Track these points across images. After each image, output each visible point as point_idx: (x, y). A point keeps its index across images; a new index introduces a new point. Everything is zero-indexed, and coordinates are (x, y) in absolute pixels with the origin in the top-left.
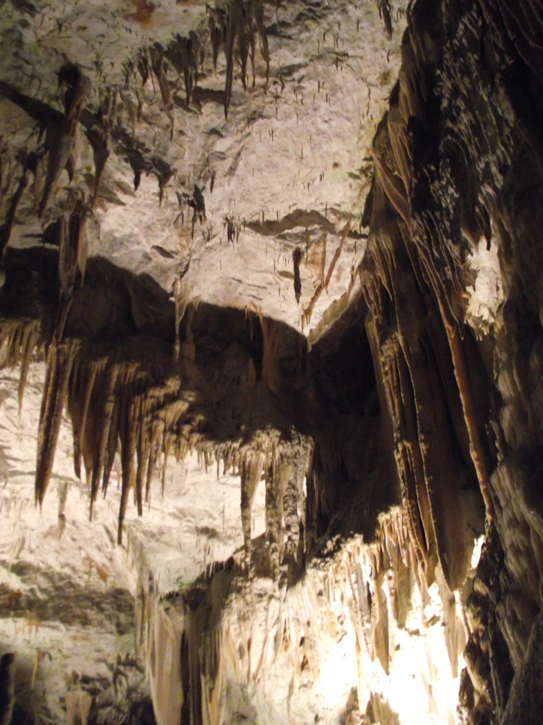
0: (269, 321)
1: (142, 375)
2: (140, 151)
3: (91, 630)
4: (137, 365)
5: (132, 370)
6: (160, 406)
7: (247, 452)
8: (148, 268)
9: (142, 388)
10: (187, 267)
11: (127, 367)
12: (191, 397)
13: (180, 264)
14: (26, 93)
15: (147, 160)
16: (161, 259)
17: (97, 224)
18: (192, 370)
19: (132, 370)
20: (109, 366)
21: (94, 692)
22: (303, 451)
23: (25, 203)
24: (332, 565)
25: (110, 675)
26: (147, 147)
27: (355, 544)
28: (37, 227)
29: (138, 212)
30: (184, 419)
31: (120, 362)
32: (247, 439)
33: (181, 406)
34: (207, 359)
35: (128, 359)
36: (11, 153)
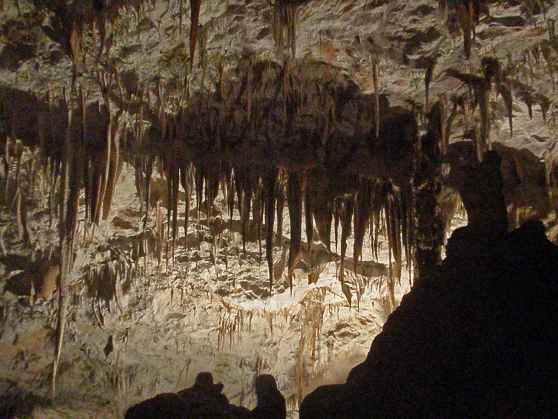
1: (534, 213)
2: (529, 92)
4: (531, 208)
5: (528, 211)
8: (527, 146)
10: (554, 145)
11: (525, 209)
13: (549, 144)
14: (463, 72)
15: (534, 96)
16: (538, 143)
17: (497, 127)
19: (528, 211)
20: (514, 209)
23: (455, 121)
26: (533, 88)
28: (461, 132)
29: (524, 120)
31: (520, 207)
35: (523, 205)
36: (448, 98)
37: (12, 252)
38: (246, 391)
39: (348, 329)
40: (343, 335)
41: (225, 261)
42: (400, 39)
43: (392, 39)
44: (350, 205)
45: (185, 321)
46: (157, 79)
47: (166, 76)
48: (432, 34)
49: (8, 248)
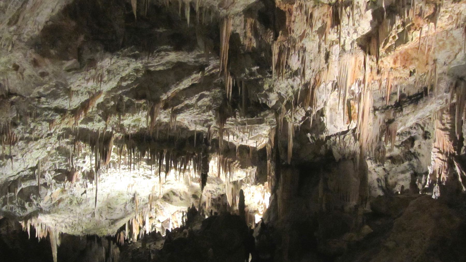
0: (251, 147)
3: (213, 185)
6: (235, 165)
7: (247, 170)
9: (232, 162)
12: (239, 162)
18: (239, 157)
21: (212, 193)
22: (255, 169)
25: (215, 191)
27: (261, 185)
30: (238, 166)
32: (247, 168)
33: (238, 164)
37: (60, 168)
38: (128, 202)
40: (168, 184)
41: (139, 169)
42: (203, 120)
43: (200, 121)
44: (183, 159)
46: (129, 125)
47: (133, 124)
48: (211, 120)
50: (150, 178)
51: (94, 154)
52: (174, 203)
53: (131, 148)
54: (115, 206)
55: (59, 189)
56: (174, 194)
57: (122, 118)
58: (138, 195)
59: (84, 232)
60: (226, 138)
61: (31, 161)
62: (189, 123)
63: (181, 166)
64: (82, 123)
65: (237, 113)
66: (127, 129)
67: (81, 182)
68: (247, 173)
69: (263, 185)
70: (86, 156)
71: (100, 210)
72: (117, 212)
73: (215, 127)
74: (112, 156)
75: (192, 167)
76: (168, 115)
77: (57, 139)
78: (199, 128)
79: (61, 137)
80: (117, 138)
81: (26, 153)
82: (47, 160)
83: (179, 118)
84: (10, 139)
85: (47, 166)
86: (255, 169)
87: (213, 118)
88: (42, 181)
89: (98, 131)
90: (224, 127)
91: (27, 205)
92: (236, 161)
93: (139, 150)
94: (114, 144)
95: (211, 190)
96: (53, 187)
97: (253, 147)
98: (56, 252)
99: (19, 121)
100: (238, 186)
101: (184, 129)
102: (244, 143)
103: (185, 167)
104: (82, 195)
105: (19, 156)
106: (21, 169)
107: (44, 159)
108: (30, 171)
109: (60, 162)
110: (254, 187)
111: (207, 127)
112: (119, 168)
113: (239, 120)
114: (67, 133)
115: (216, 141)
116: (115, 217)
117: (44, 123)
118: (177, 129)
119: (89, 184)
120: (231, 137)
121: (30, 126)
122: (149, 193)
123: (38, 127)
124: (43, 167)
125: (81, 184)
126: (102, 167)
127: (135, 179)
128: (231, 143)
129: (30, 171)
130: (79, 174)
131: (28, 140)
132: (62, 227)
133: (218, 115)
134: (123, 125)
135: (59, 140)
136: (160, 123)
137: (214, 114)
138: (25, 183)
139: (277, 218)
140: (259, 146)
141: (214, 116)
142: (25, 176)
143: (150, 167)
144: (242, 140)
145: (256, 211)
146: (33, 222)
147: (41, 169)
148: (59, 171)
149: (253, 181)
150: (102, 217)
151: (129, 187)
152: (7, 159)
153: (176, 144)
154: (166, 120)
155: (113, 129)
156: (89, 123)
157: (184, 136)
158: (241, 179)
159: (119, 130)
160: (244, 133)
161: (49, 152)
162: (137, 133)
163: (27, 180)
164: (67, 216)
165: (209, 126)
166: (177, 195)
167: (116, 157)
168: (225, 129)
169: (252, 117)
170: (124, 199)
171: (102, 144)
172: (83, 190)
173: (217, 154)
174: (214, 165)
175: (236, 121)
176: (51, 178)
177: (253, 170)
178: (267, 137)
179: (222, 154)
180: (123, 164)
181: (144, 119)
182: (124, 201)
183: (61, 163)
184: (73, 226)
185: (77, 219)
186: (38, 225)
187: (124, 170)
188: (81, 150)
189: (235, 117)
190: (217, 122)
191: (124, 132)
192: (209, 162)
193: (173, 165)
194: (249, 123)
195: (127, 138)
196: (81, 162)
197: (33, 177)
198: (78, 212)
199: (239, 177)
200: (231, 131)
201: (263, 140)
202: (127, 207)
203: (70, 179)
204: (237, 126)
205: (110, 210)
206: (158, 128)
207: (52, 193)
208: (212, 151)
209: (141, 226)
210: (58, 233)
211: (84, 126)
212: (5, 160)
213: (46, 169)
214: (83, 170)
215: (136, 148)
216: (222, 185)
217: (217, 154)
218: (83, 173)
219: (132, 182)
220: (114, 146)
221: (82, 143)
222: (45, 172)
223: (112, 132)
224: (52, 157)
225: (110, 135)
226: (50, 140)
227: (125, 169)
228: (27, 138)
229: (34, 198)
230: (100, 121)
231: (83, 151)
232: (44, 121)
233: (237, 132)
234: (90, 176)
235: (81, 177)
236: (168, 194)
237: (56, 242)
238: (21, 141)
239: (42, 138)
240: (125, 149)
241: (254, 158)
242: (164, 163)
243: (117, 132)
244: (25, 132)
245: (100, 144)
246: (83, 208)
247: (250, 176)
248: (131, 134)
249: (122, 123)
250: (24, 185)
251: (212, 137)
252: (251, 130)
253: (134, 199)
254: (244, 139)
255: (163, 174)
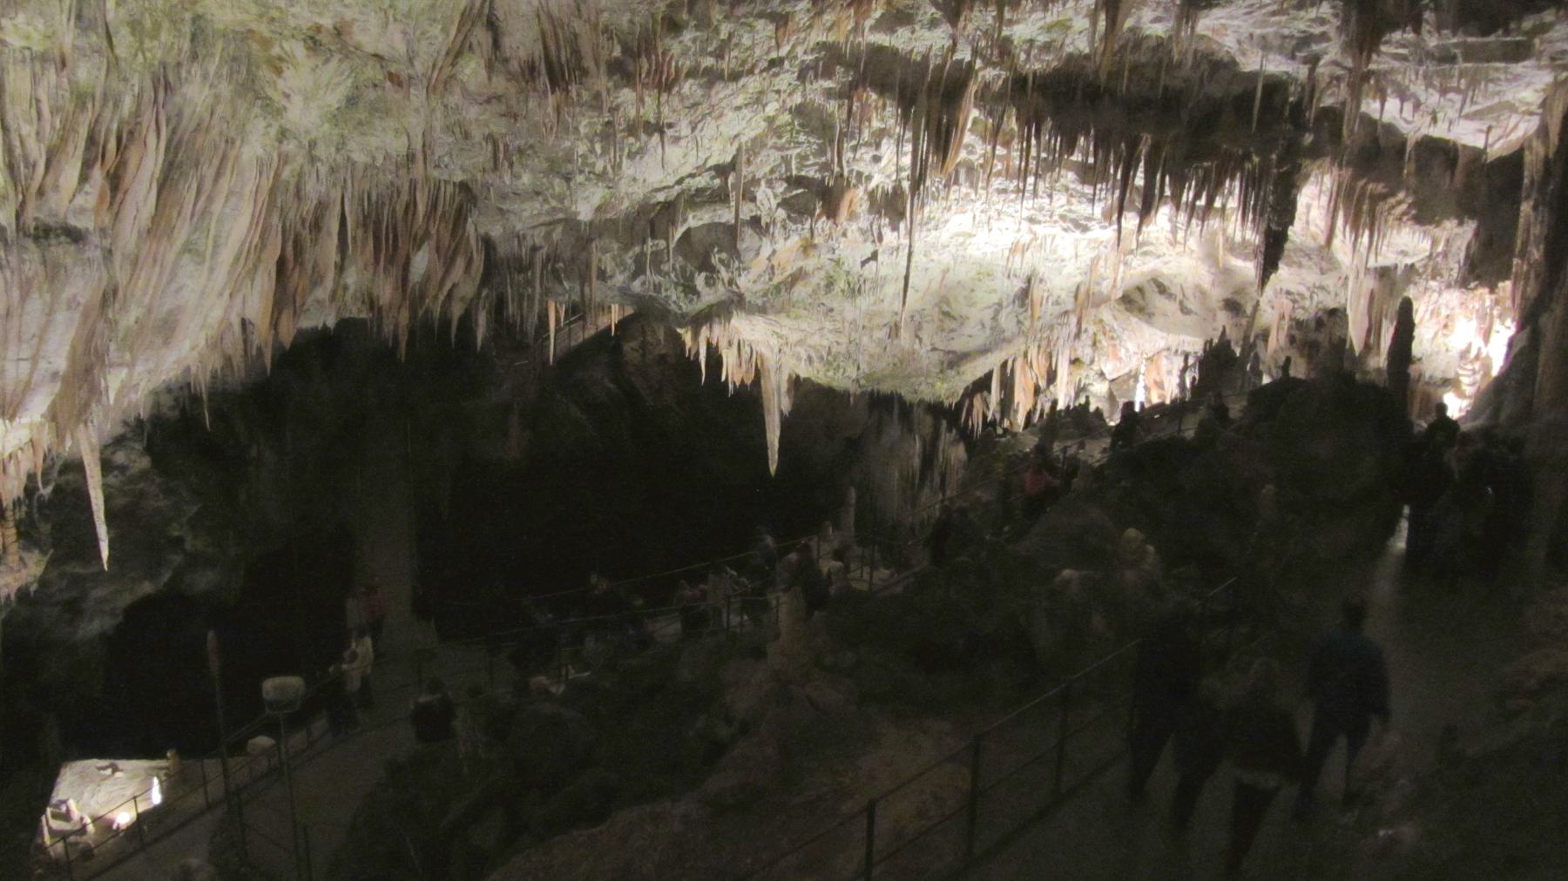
0: (1465, 147)
3: (1304, 271)
6: (1393, 207)
7: (1437, 232)
9: (1384, 197)
12: (1410, 200)
18: (1413, 181)
21: (1294, 301)
22: (1470, 227)
24: (1471, 295)
25: (1307, 294)
27: (1484, 291)
30: (1404, 213)
32: (1438, 224)
34: (1422, 169)
35: (1378, 181)
39: (1150, 248)
40: (1145, 254)
41: (1050, 196)
42: (1292, 37)
43: (1284, 37)
44: (1207, 171)
45: (973, 240)
46: (1031, 42)
47: (1042, 39)
48: (1324, 37)
49: (799, 169)
50: (1085, 229)
51: (909, 135)
52: (1158, 320)
53: (1031, 121)
54: (965, 311)
55: (795, 240)
56: (1162, 289)
57: (1007, 15)
58: (1041, 281)
59: (862, 382)
60: (1371, 107)
61: (717, 146)
62: (1239, 42)
63: (1197, 196)
64: (873, 29)
65: (1428, 15)
66: (1023, 56)
67: (863, 223)
68: (1434, 243)
69: (1492, 291)
70: (884, 141)
71: (917, 318)
72: (967, 330)
73: (1336, 63)
74: (967, 147)
75: (1233, 203)
76: (1166, 10)
77: (799, 78)
78: (1277, 66)
79: (811, 73)
80: (987, 86)
81: (704, 116)
82: (764, 145)
83: (1207, 23)
84: (659, 71)
85: (765, 163)
86: (1470, 227)
87: (1330, 30)
88: (747, 211)
89: (926, 57)
90: (1372, 66)
91: (700, 280)
92: (1401, 195)
93: (1058, 129)
94: (976, 106)
95: (1293, 288)
96: (777, 231)
97: (1474, 149)
98: (778, 433)
99: (685, 16)
100: (1394, 284)
101: (1220, 66)
102: (1439, 132)
103: (1210, 201)
104: (864, 263)
105: (684, 128)
106: (688, 169)
107: (754, 140)
108: (713, 178)
109: (804, 156)
110: (1453, 297)
111: (1305, 61)
112: (986, 188)
113: (1432, 42)
114: (830, 58)
115: (1332, 117)
116: (959, 345)
117: (760, 24)
118: (1196, 64)
119: (887, 232)
120: (1392, 104)
121: (717, 30)
122: (1079, 279)
123: (741, 37)
124: (751, 168)
125: (862, 232)
126: (933, 181)
127: (1035, 227)
128: (1390, 129)
129: (713, 178)
130: (857, 198)
131: (712, 78)
132: (799, 359)
133: (1353, 19)
134: (1008, 40)
135: (803, 82)
136: (1138, 41)
137: (1336, 16)
138: (699, 214)
139: (1527, 412)
140: (1497, 146)
141: (1336, 22)
142: (699, 191)
143: (1088, 190)
144: (1434, 120)
145: (1449, 383)
146: (716, 333)
147: (746, 171)
148: (797, 182)
149: (1455, 274)
150: (921, 340)
151: (1013, 251)
152: (650, 135)
153: (1185, 116)
154: (1159, 30)
155: (975, 52)
156: (900, 31)
157: (1215, 90)
158: (1409, 261)
159: (994, 59)
160: (1444, 91)
161: (770, 120)
162: (1055, 70)
163: (703, 204)
164: (816, 326)
165: (1313, 61)
166: (1171, 296)
167: (981, 148)
168: (1372, 73)
169: (1485, 33)
170: (994, 291)
171: (936, 102)
172: (868, 249)
173: (1332, 164)
174: (1313, 201)
175: (1417, 46)
176: (774, 203)
177: (1459, 235)
178: (1531, 114)
179: (1348, 164)
180: (999, 174)
181: (1081, 23)
182: (995, 298)
183: (806, 158)
184: (830, 359)
185: (844, 340)
186: (730, 344)
187: (1003, 197)
188: (869, 120)
189: (1417, 31)
190: (1347, 47)
191: (1013, 68)
192: (1299, 188)
193: (1168, 192)
194: (1471, 54)
195: (1019, 85)
196: (868, 157)
197: (719, 197)
198: (849, 316)
199: (1404, 253)
200: (1394, 83)
201: (1515, 127)
202: (1003, 317)
203: (831, 212)
204: (1420, 63)
205: (949, 324)
206: (1130, 58)
207: (774, 252)
208: (1315, 153)
209: (1042, 384)
210: (785, 377)
211: (882, 39)
212: (644, 137)
213: (759, 175)
214: (872, 185)
215: (1049, 124)
216: (1334, 275)
217: (1332, 164)
218: (872, 195)
219: (1026, 238)
220: (975, 113)
221: (874, 96)
222: (755, 182)
223: (970, 65)
224: (780, 137)
225: (964, 74)
226: (776, 80)
227: (1005, 191)
228: (708, 71)
229: (721, 261)
230: (933, 24)
231: (876, 124)
232: (761, 15)
233: (1418, 88)
234: (891, 206)
235: (866, 205)
236: (1140, 289)
237: (777, 404)
238: (691, 81)
239: (751, 72)
240: (1012, 124)
241: (1469, 187)
242: (1139, 181)
243: (988, 63)
244: (703, 52)
245: (930, 101)
246: (864, 307)
247: (1445, 255)
248: (1035, 73)
249: (1006, 32)
250: (695, 220)
251: (1319, 100)
252: (1473, 83)
253: (1024, 295)
254: (1440, 116)
255: (1130, 220)
